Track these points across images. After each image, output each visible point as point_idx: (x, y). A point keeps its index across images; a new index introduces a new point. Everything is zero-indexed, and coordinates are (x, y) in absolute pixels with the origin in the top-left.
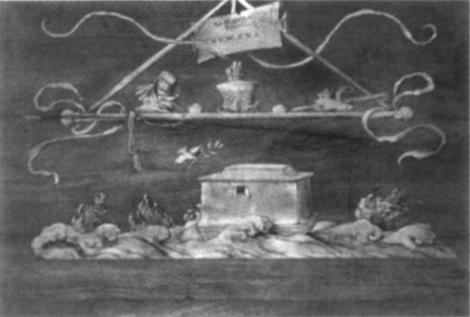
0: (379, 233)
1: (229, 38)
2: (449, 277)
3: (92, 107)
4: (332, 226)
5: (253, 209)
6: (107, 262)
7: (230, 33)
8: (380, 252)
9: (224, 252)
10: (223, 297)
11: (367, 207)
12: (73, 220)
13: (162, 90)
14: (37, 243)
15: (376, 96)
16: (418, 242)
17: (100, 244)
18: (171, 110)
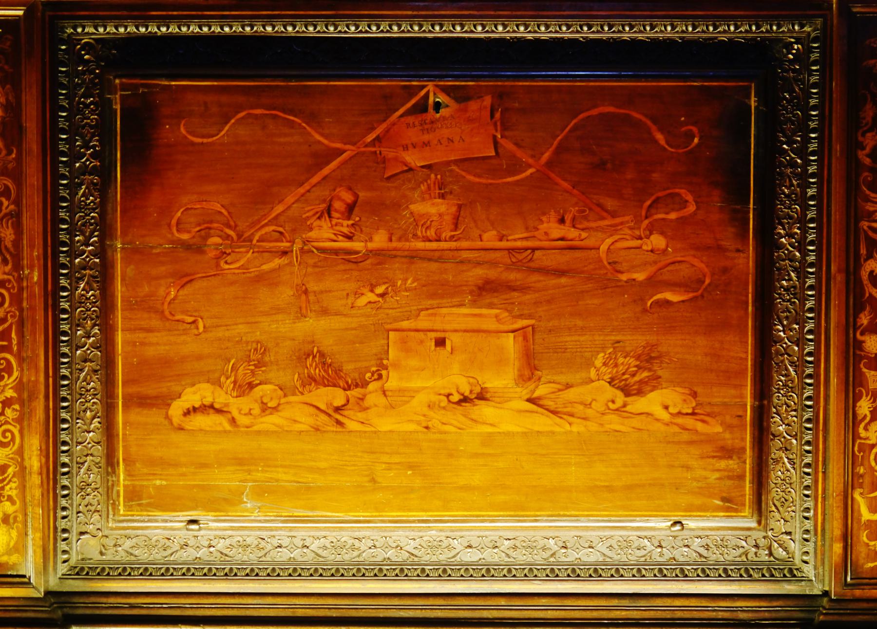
0: (620, 398)
1: (426, 144)
2: (714, 457)
3: (246, 235)
4: (560, 390)
5: (456, 368)
6: (266, 433)
7: (426, 137)
8: (622, 424)
9: (419, 423)
10: (418, 482)
11: (605, 364)
12: (223, 379)
13: (336, 211)
14: (176, 409)
15: (618, 220)
16: (672, 410)
17: (257, 411)
18: (349, 238)
